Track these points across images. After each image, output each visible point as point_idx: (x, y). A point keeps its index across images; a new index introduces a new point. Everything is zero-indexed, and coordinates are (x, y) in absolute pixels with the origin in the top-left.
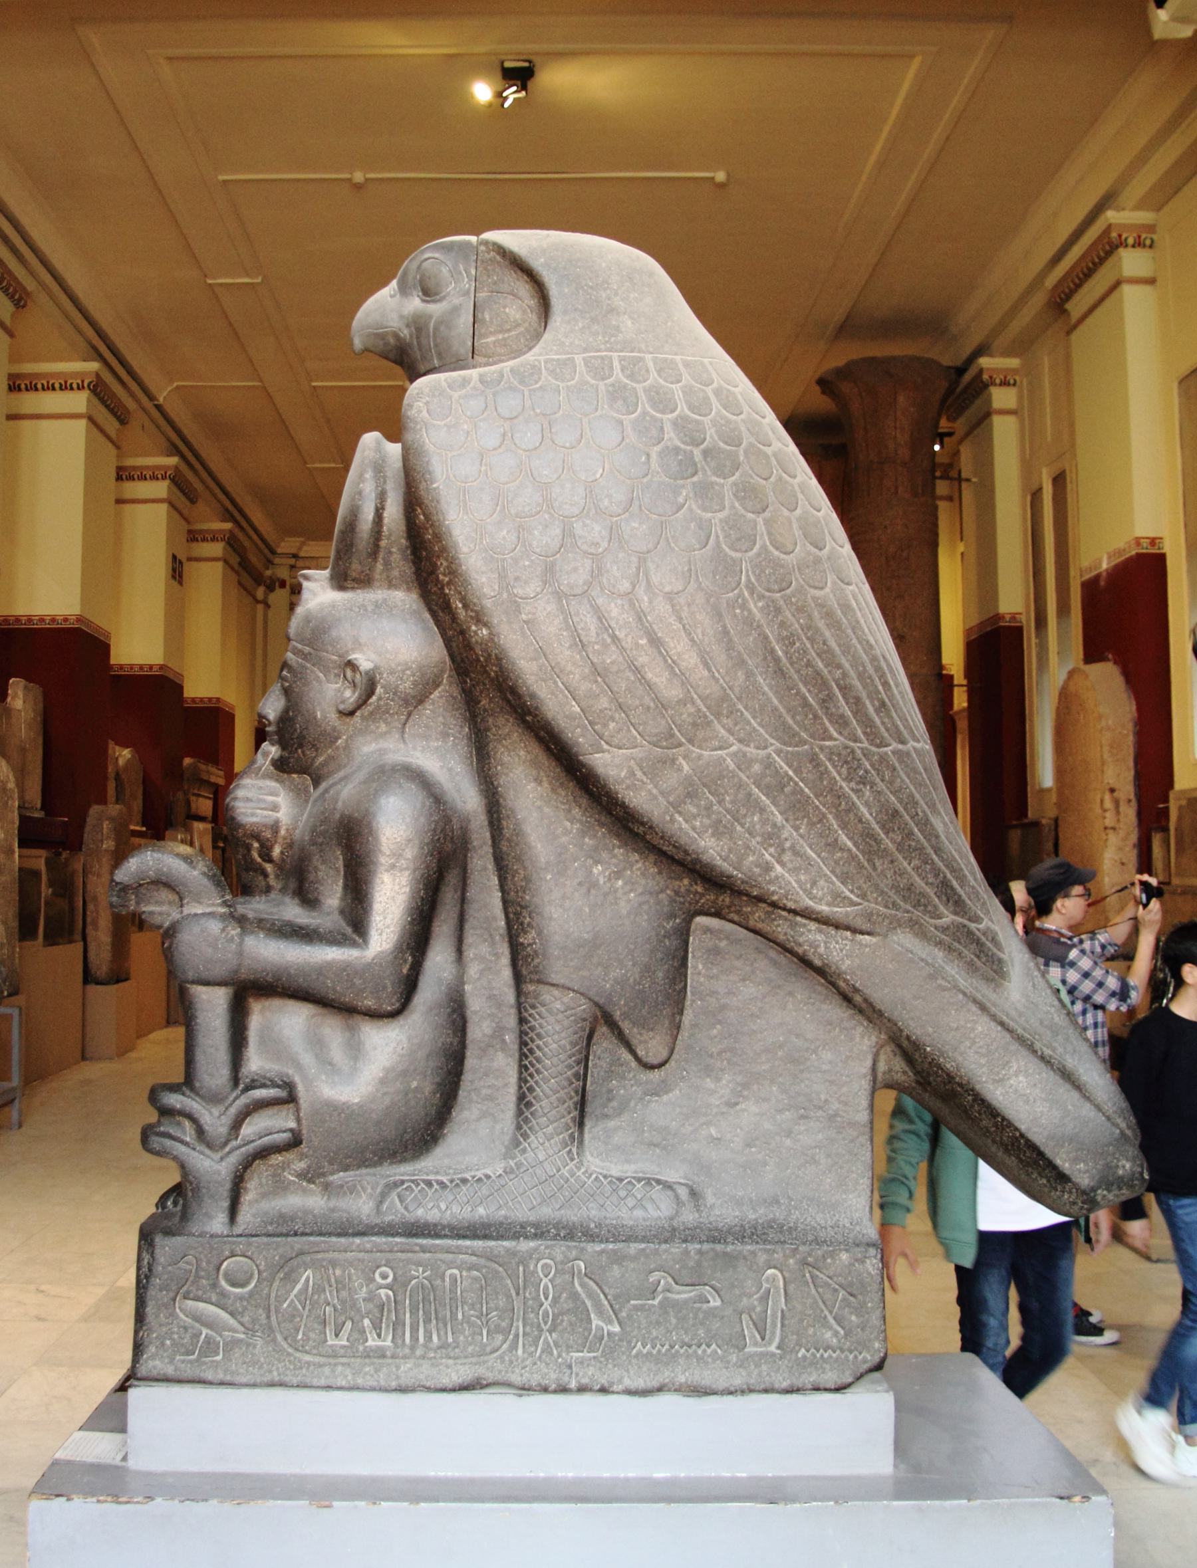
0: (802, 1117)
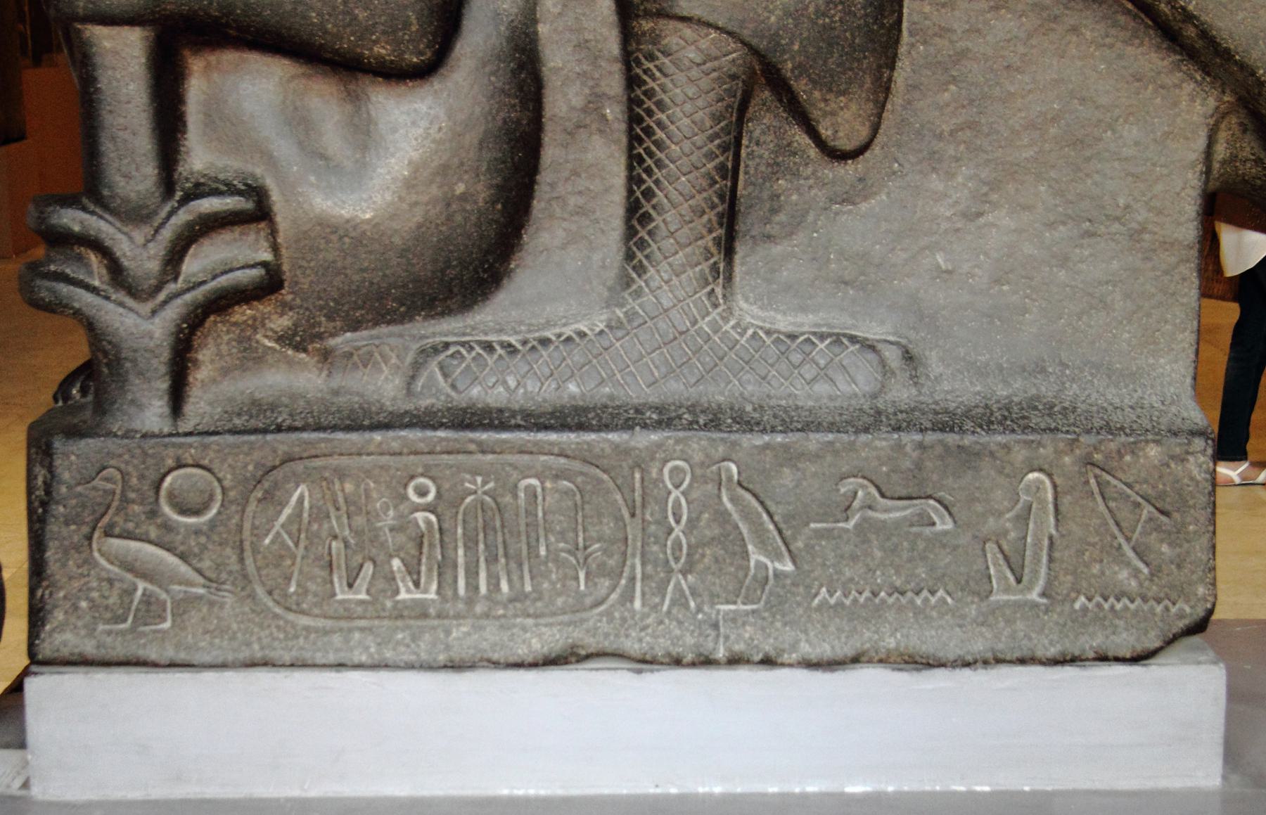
0: (1089, 234)
